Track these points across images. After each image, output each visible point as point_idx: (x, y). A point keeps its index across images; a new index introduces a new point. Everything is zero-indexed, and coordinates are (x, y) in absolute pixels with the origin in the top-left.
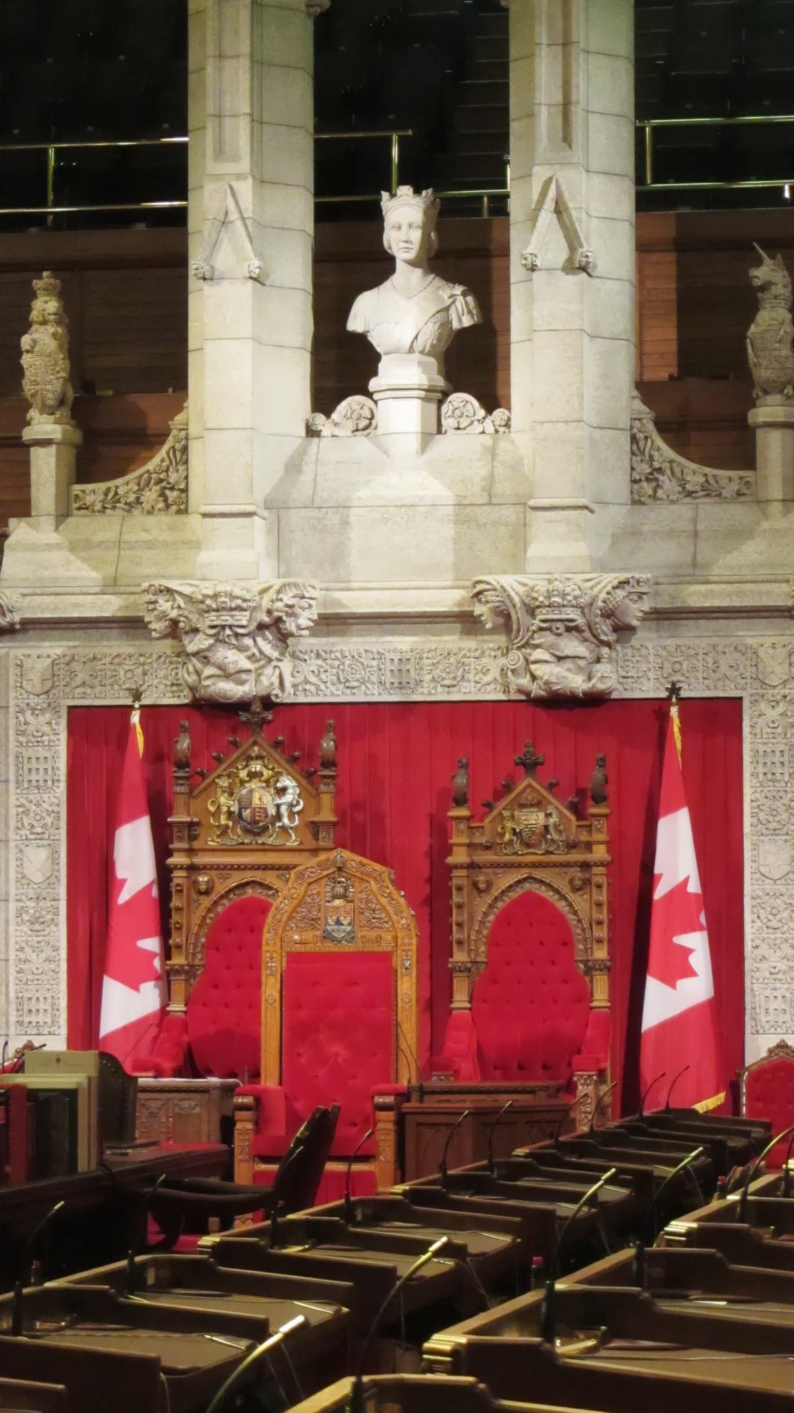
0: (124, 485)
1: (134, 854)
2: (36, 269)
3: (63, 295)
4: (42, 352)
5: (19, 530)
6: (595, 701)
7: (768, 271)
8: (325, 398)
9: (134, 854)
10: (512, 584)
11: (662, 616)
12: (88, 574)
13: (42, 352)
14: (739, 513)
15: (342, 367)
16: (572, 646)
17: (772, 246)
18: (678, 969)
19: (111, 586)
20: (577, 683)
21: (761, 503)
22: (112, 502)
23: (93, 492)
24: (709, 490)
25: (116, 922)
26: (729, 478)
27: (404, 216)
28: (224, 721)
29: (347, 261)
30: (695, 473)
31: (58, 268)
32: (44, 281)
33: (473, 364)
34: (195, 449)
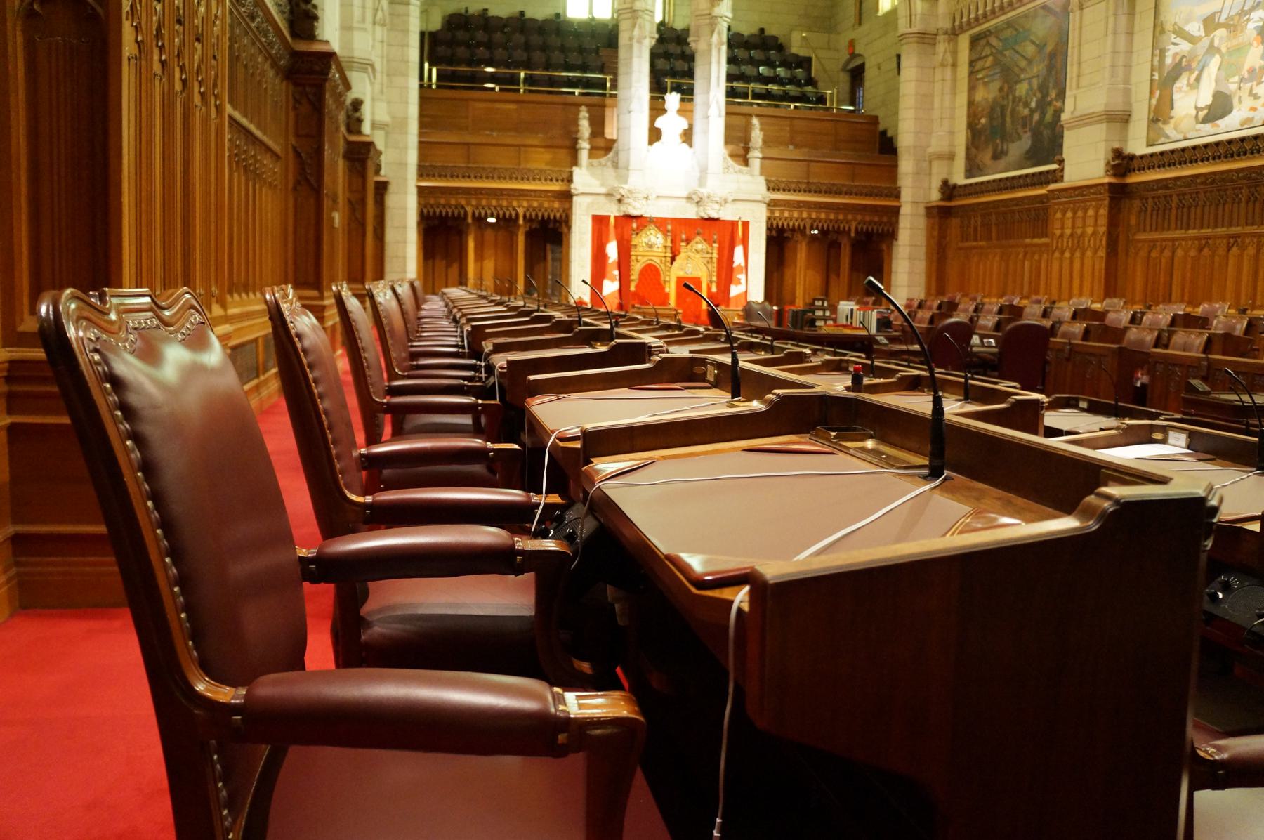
0: (603, 160)
1: (612, 250)
2: (580, 105)
3: (588, 112)
4: (585, 127)
5: (576, 170)
6: (717, 220)
7: (755, 121)
8: (651, 142)
9: (612, 250)
10: (704, 191)
11: (734, 200)
12: (598, 183)
13: (585, 127)
14: (748, 178)
15: (655, 135)
16: (717, 206)
17: (757, 116)
18: (739, 282)
19: (602, 185)
20: (715, 215)
21: (752, 175)
22: (600, 164)
23: (595, 162)
24: (740, 171)
25: (609, 269)
26: (744, 168)
27: (672, 99)
28: (641, 222)
29: (657, 109)
30: (738, 167)
31: (587, 105)
32: (583, 108)
33: (688, 136)
34: (622, 156)
